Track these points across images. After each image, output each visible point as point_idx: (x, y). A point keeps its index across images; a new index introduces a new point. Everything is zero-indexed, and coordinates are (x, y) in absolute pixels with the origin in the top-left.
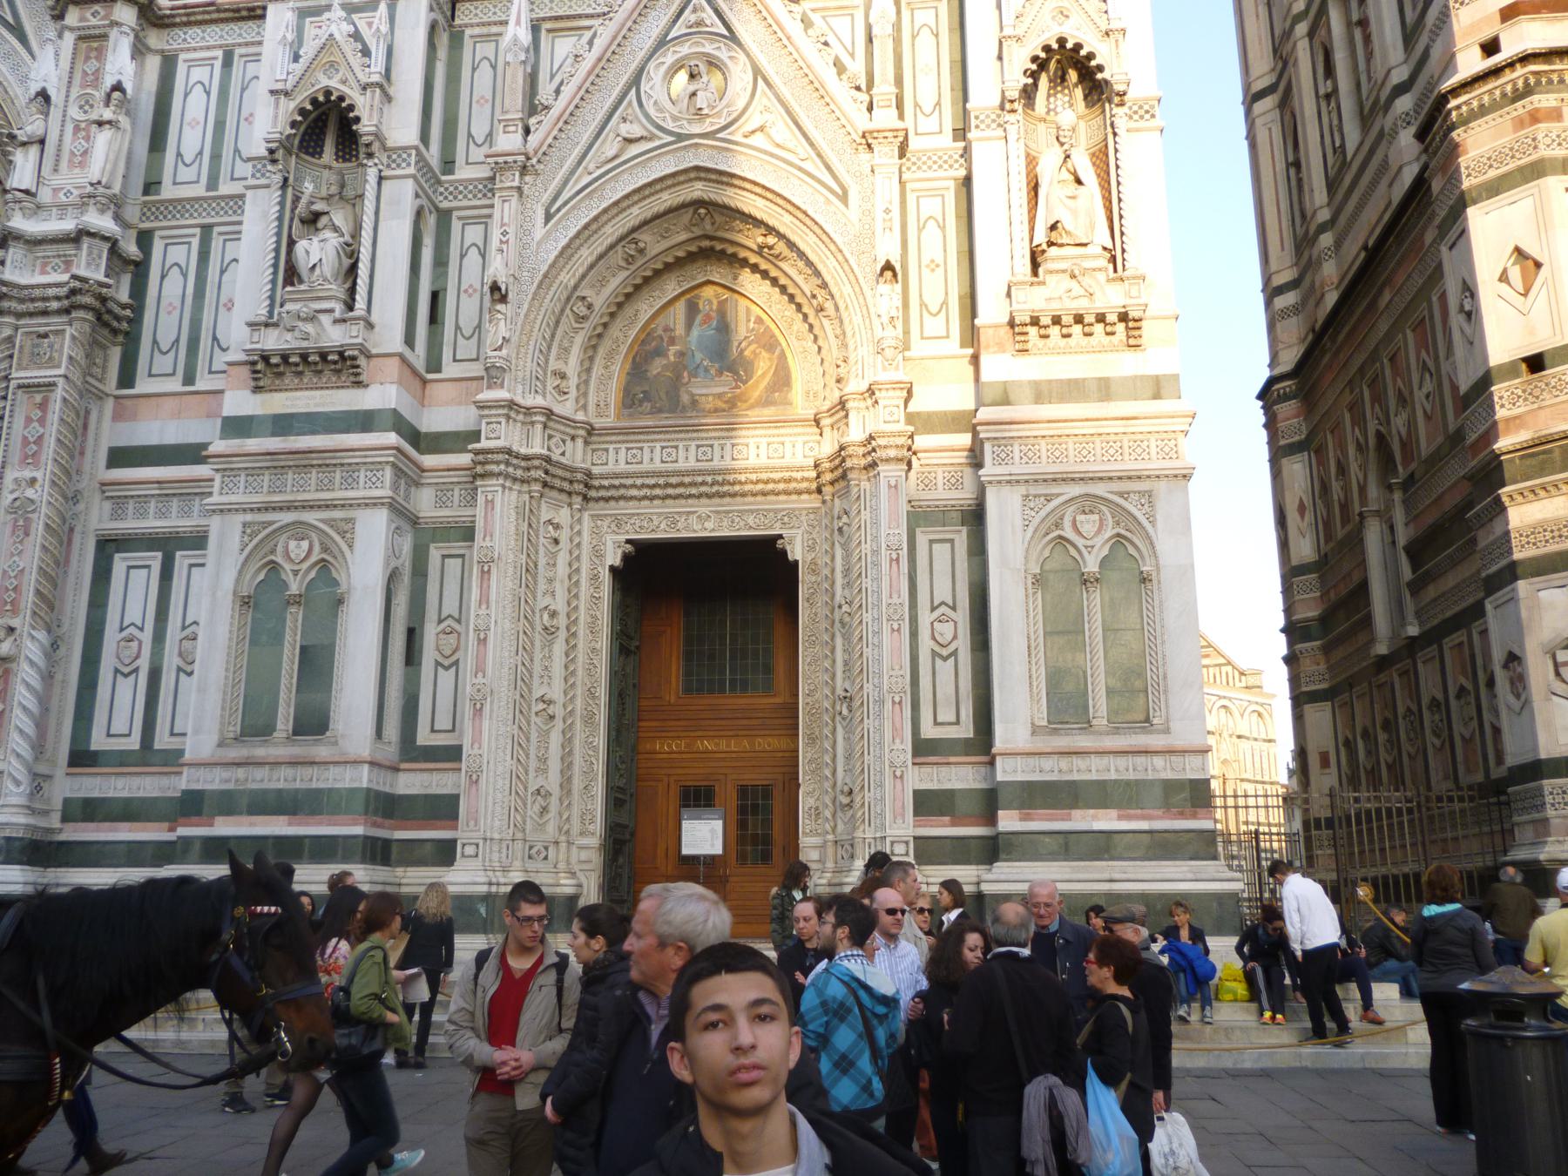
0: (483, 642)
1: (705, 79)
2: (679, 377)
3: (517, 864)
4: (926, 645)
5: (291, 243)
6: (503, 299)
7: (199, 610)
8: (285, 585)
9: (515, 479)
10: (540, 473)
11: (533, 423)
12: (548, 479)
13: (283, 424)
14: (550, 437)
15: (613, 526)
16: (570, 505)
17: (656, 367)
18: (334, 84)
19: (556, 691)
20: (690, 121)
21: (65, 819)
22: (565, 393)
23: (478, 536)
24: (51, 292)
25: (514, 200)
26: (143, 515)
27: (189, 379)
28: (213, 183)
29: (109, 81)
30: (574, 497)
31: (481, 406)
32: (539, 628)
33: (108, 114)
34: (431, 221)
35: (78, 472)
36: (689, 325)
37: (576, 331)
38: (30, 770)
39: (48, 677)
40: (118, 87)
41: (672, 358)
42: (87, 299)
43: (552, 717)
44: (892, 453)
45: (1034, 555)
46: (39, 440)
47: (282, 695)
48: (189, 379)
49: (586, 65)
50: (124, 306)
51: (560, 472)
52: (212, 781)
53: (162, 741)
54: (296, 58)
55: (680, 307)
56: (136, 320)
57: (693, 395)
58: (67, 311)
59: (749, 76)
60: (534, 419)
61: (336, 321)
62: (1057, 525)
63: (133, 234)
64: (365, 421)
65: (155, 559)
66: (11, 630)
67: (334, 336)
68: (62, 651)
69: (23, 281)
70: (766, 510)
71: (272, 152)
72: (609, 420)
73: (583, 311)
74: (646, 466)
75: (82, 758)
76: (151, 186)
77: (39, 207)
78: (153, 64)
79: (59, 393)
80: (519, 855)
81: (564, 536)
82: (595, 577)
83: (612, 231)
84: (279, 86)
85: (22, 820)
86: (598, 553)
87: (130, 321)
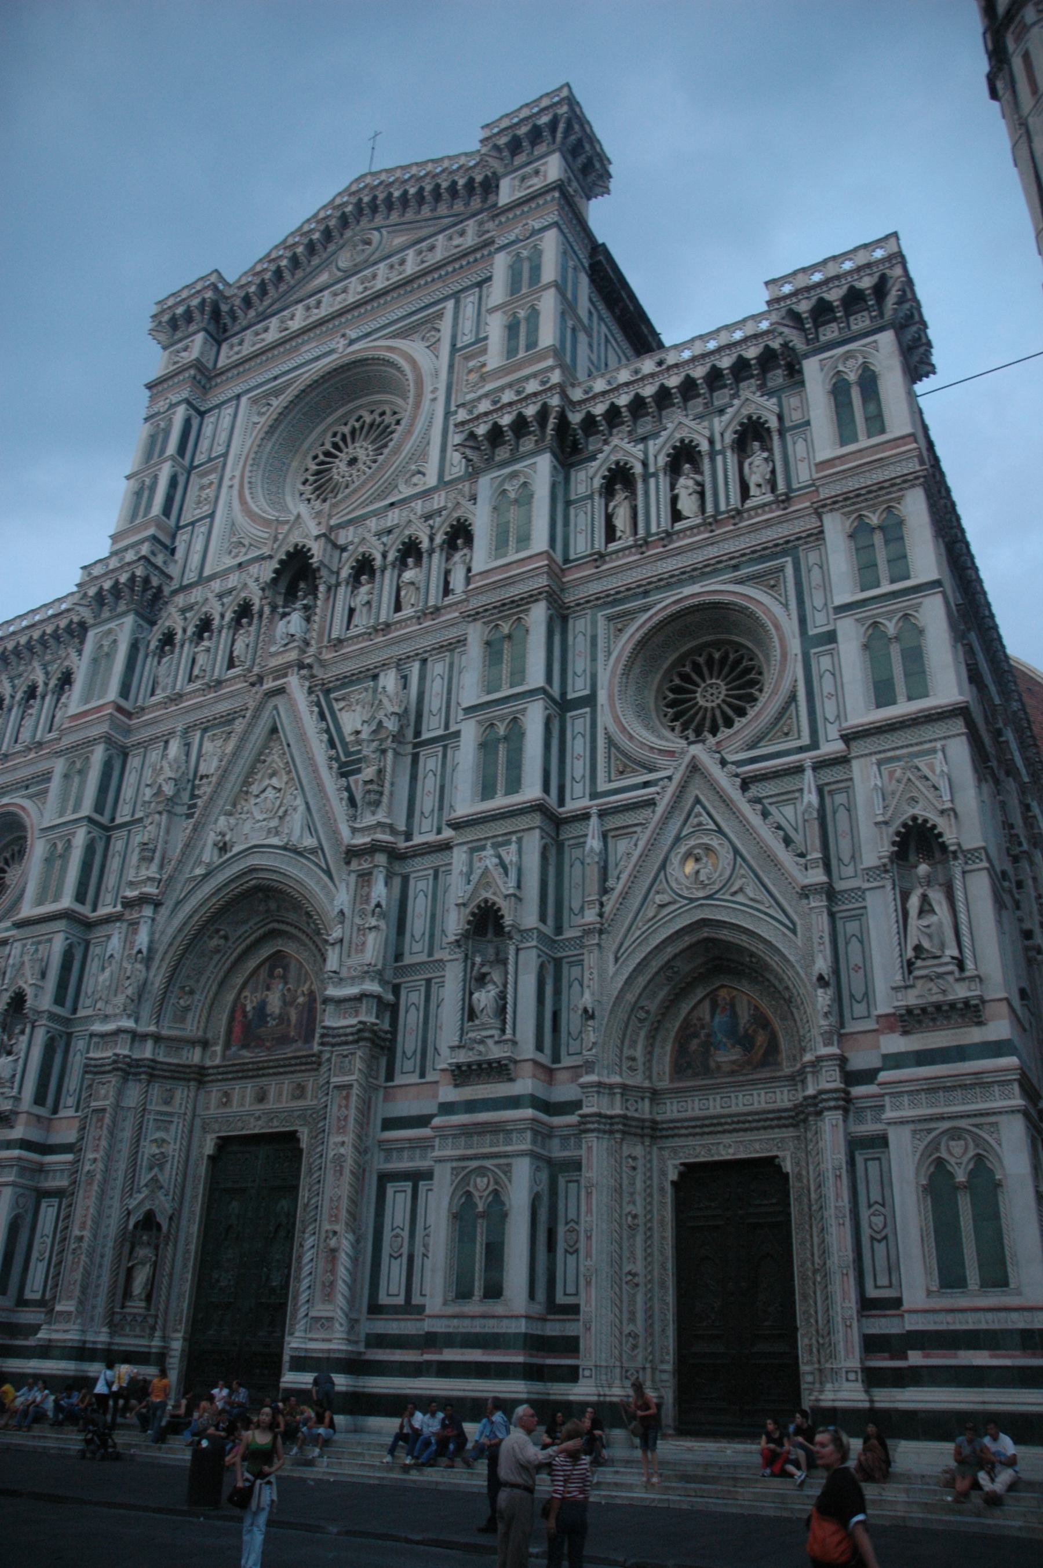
0: (589, 1238)
1: (705, 859)
3: (617, 1382)
4: (866, 1232)
5: (471, 994)
6: (592, 1017)
7: (431, 1220)
8: (476, 1205)
9: (605, 1132)
10: (621, 1127)
13: (471, 1106)
16: (643, 1143)
17: (694, 1045)
18: (488, 895)
19: (639, 1267)
20: (697, 889)
21: (368, 1345)
23: (584, 1169)
24: (349, 1030)
25: (596, 952)
26: (401, 1160)
27: (422, 1075)
28: (430, 954)
29: (373, 903)
31: (583, 1086)
32: (625, 1227)
33: (373, 922)
34: (550, 968)
35: (367, 1135)
36: (712, 1017)
37: (640, 1028)
38: (347, 1316)
39: (355, 1260)
40: (378, 905)
42: (367, 1035)
43: (637, 1285)
44: (832, 1104)
45: (923, 1170)
46: (346, 1118)
47: (477, 1275)
48: (422, 1075)
49: (634, 859)
50: (386, 1032)
51: (634, 1123)
52: (439, 1327)
53: (416, 1300)
54: (469, 882)
55: (707, 1004)
56: (394, 1040)
58: (356, 1041)
59: (731, 856)
61: (497, 1043)
62: (937, 1149)
63: (390, 988)
64: (514, 1102)
65: (408, 1185)
66: (335, 1233)
67: (496, 1052)
68: (362, 1245)
69: (335, 1025)
71: (457, 941)
72: (665, 1084)
75: (375, 1309)
76: (399, 956)
77: (341, 979)
78: (397, 882)
79: (355, 1090)
80: (618, 1376)
81: (640, 1163)
82: (662, 1189)
83: (656, 964)
84: (460, 901)
85: (344, 1347)
86: (663, 1173)
87: (390, 1041)
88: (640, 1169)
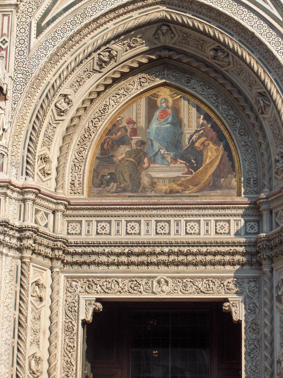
2: (140, 162)
11: (24, 201)
12: (36, 247)
14: (37, 211)
15: (85, 286)
16: (51, 269)
22: (48, 174)
30: (55, 261)
36: (149, 120)
41: (134, 146)
51: (45, 242)
55: (143, 102)
57: (152, 178)
60: (26, 196)
70: (214, 277)
72: (83, 198)
73: (63, 106)
74: (113, 238)
81: (46, 294)
88: (47, 302)
